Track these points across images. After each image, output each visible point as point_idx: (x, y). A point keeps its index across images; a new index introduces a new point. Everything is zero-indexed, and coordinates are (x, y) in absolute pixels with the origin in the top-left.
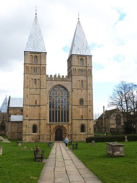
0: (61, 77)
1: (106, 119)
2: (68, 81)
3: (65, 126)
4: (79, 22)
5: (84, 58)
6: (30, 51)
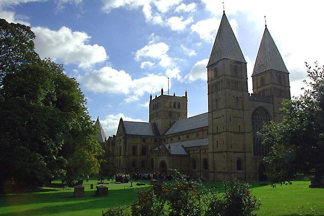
5: (282, 75)
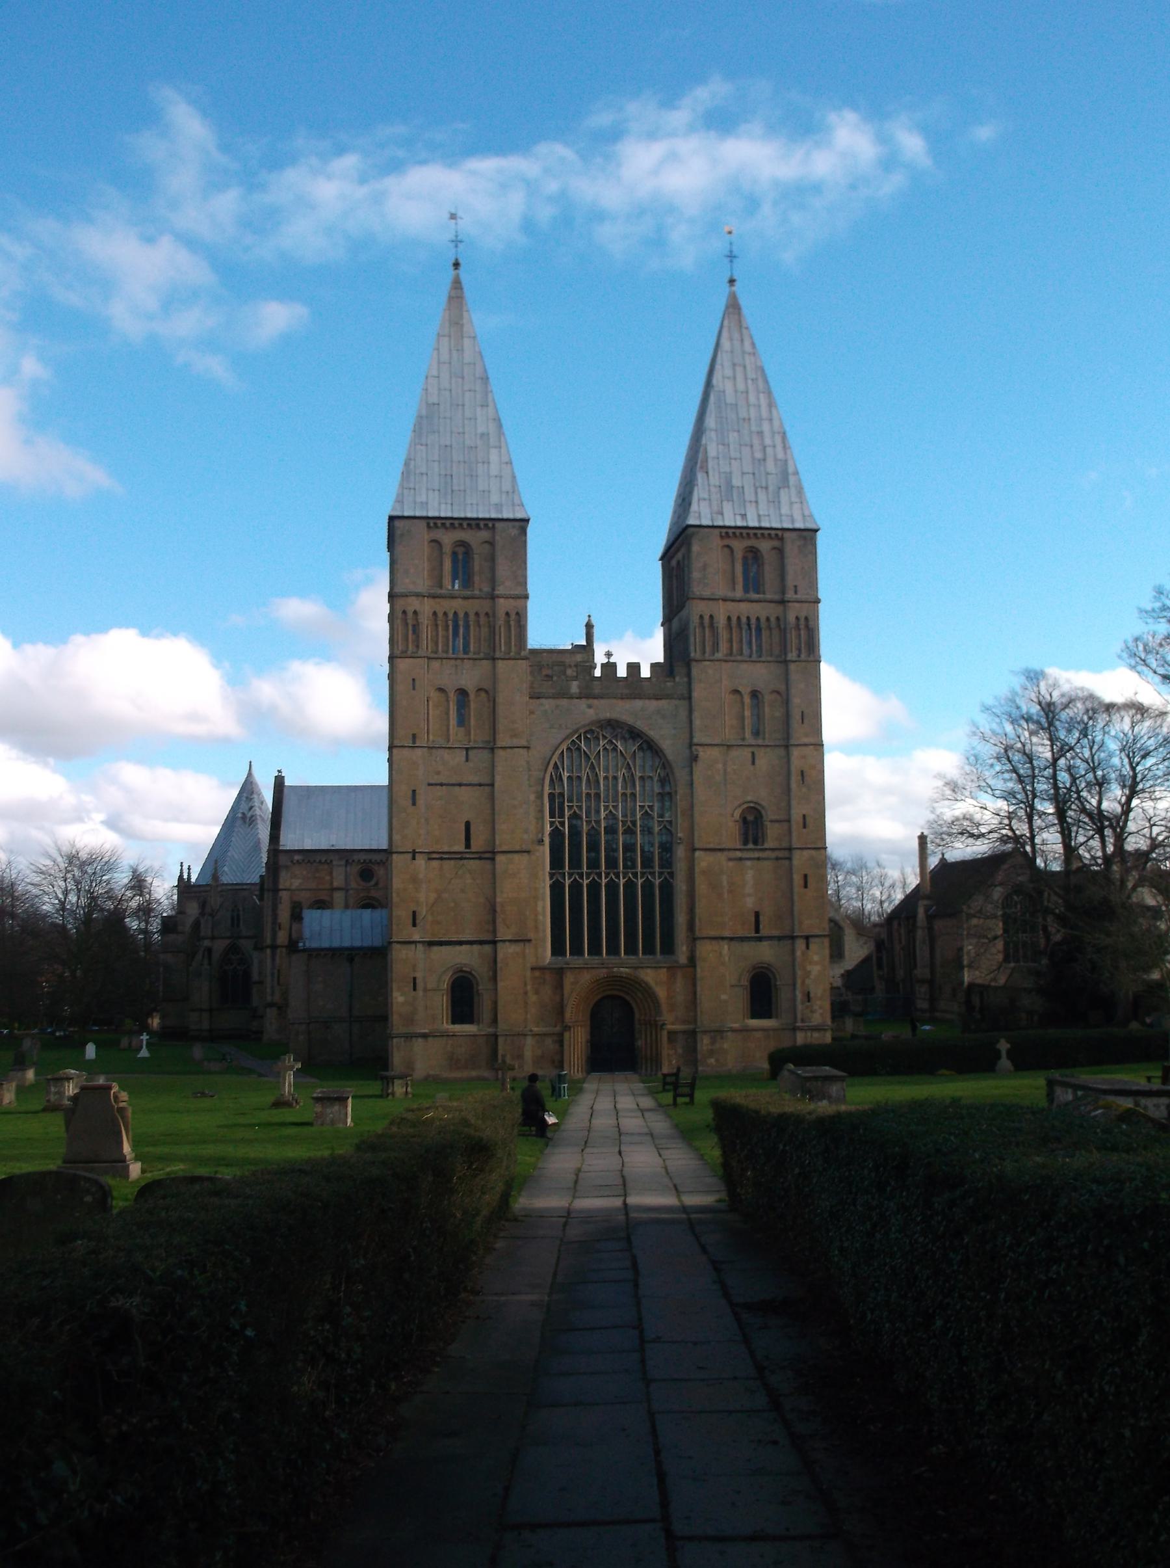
0: (622, 672)
1: (938, 924)
2: (668, 697)
3: (649, 976)
4: (733, 307)
5: (765, 546)
6: (424, 514)
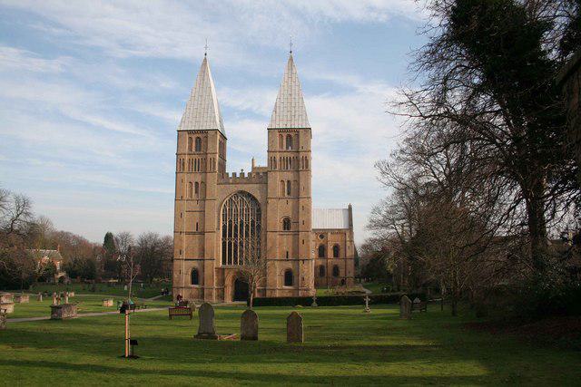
5: (292, 134)
